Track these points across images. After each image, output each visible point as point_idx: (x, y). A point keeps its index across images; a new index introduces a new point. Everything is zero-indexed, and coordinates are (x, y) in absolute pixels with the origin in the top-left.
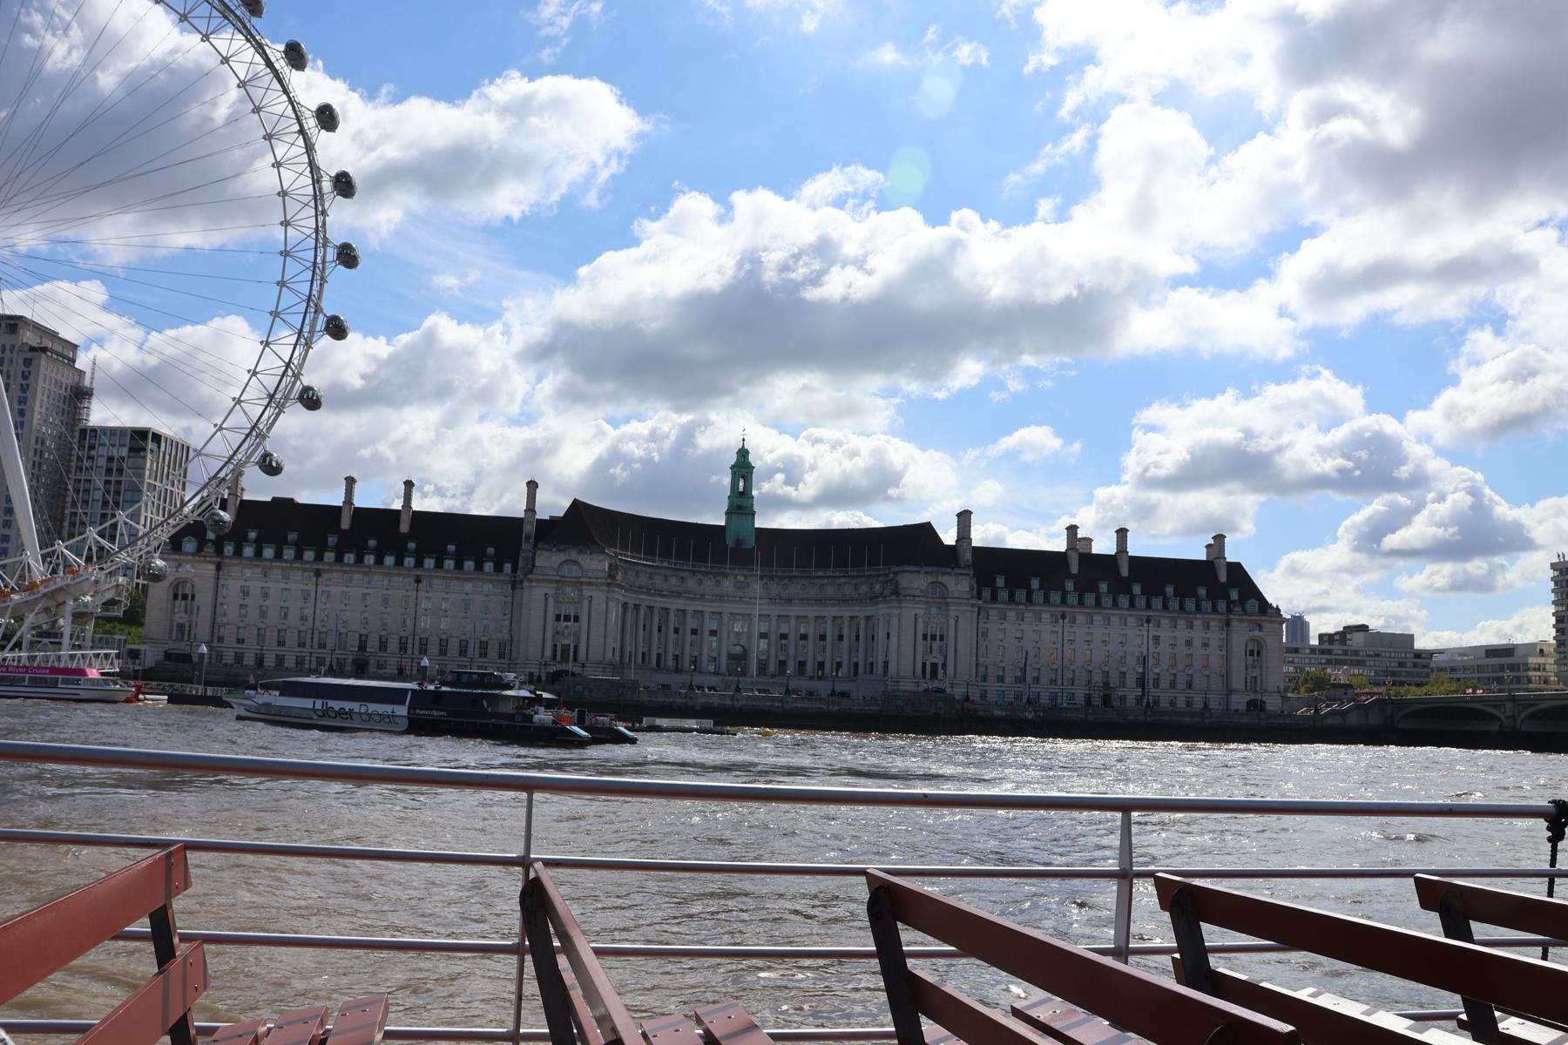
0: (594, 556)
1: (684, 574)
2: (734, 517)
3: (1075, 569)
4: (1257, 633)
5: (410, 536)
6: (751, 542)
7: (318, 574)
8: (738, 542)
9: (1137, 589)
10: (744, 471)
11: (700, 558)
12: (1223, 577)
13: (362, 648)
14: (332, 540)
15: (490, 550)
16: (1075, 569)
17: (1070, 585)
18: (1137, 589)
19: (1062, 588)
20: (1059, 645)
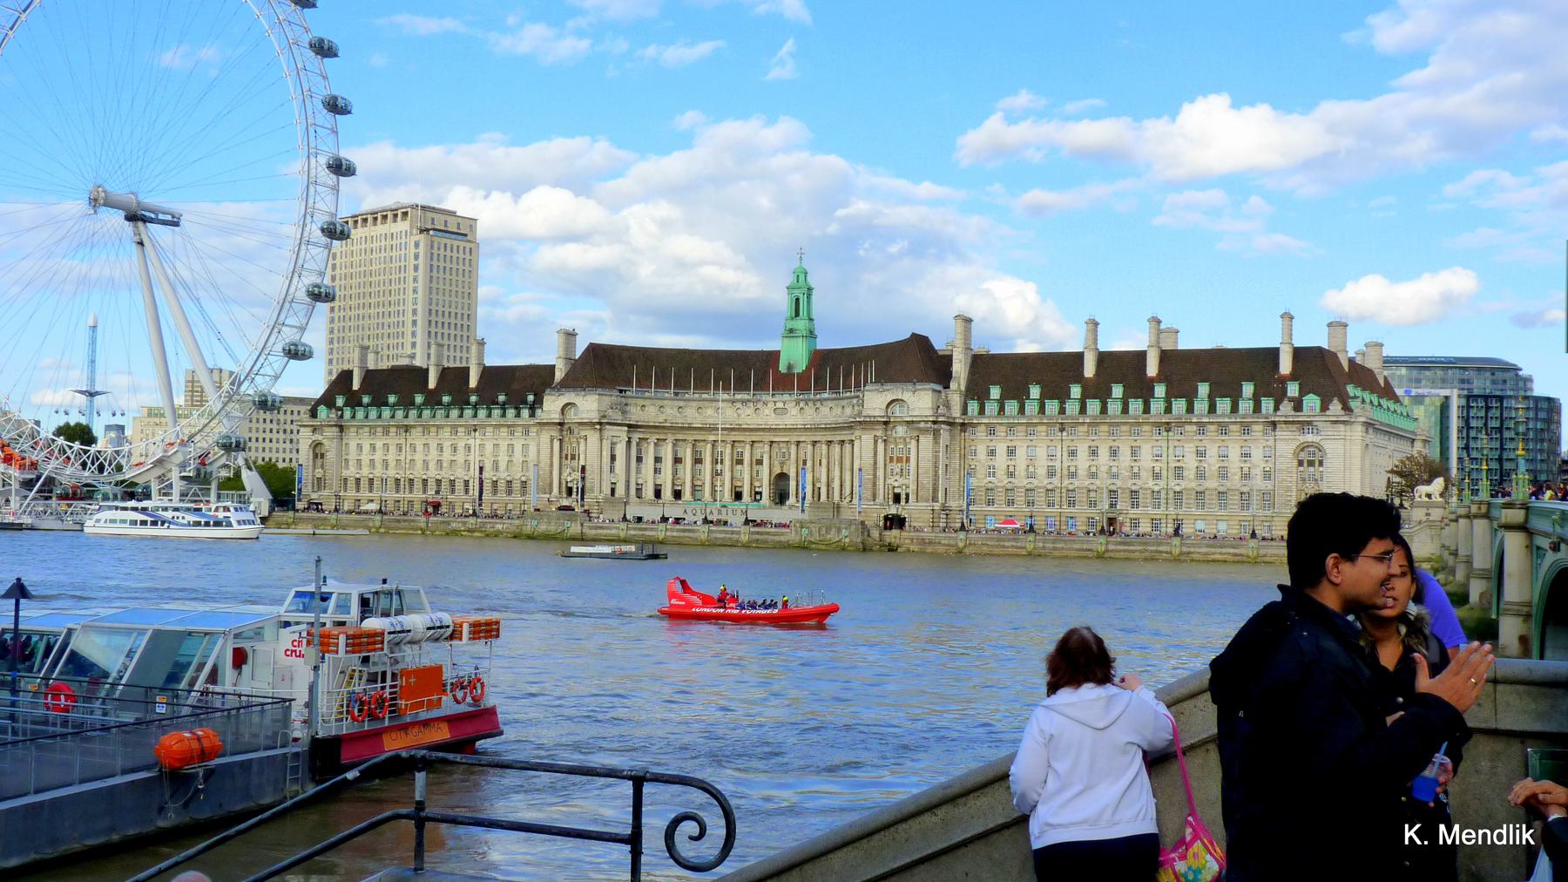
3: (1089, 370)
4: (1310, 438)
5: (476, 390)
6: (801, 365)
7: (407, 429)
8: (790, 367)
9: (1160, 390)
10: (797, 293)
11: (742, 385)
12: (1285, 366)
13: (438, 492)
14: (419, 399)
15: (531, 398)
16: (1089, 370)
17: (1076, 391)
18: (1160, 390)
19: (1063, 396)
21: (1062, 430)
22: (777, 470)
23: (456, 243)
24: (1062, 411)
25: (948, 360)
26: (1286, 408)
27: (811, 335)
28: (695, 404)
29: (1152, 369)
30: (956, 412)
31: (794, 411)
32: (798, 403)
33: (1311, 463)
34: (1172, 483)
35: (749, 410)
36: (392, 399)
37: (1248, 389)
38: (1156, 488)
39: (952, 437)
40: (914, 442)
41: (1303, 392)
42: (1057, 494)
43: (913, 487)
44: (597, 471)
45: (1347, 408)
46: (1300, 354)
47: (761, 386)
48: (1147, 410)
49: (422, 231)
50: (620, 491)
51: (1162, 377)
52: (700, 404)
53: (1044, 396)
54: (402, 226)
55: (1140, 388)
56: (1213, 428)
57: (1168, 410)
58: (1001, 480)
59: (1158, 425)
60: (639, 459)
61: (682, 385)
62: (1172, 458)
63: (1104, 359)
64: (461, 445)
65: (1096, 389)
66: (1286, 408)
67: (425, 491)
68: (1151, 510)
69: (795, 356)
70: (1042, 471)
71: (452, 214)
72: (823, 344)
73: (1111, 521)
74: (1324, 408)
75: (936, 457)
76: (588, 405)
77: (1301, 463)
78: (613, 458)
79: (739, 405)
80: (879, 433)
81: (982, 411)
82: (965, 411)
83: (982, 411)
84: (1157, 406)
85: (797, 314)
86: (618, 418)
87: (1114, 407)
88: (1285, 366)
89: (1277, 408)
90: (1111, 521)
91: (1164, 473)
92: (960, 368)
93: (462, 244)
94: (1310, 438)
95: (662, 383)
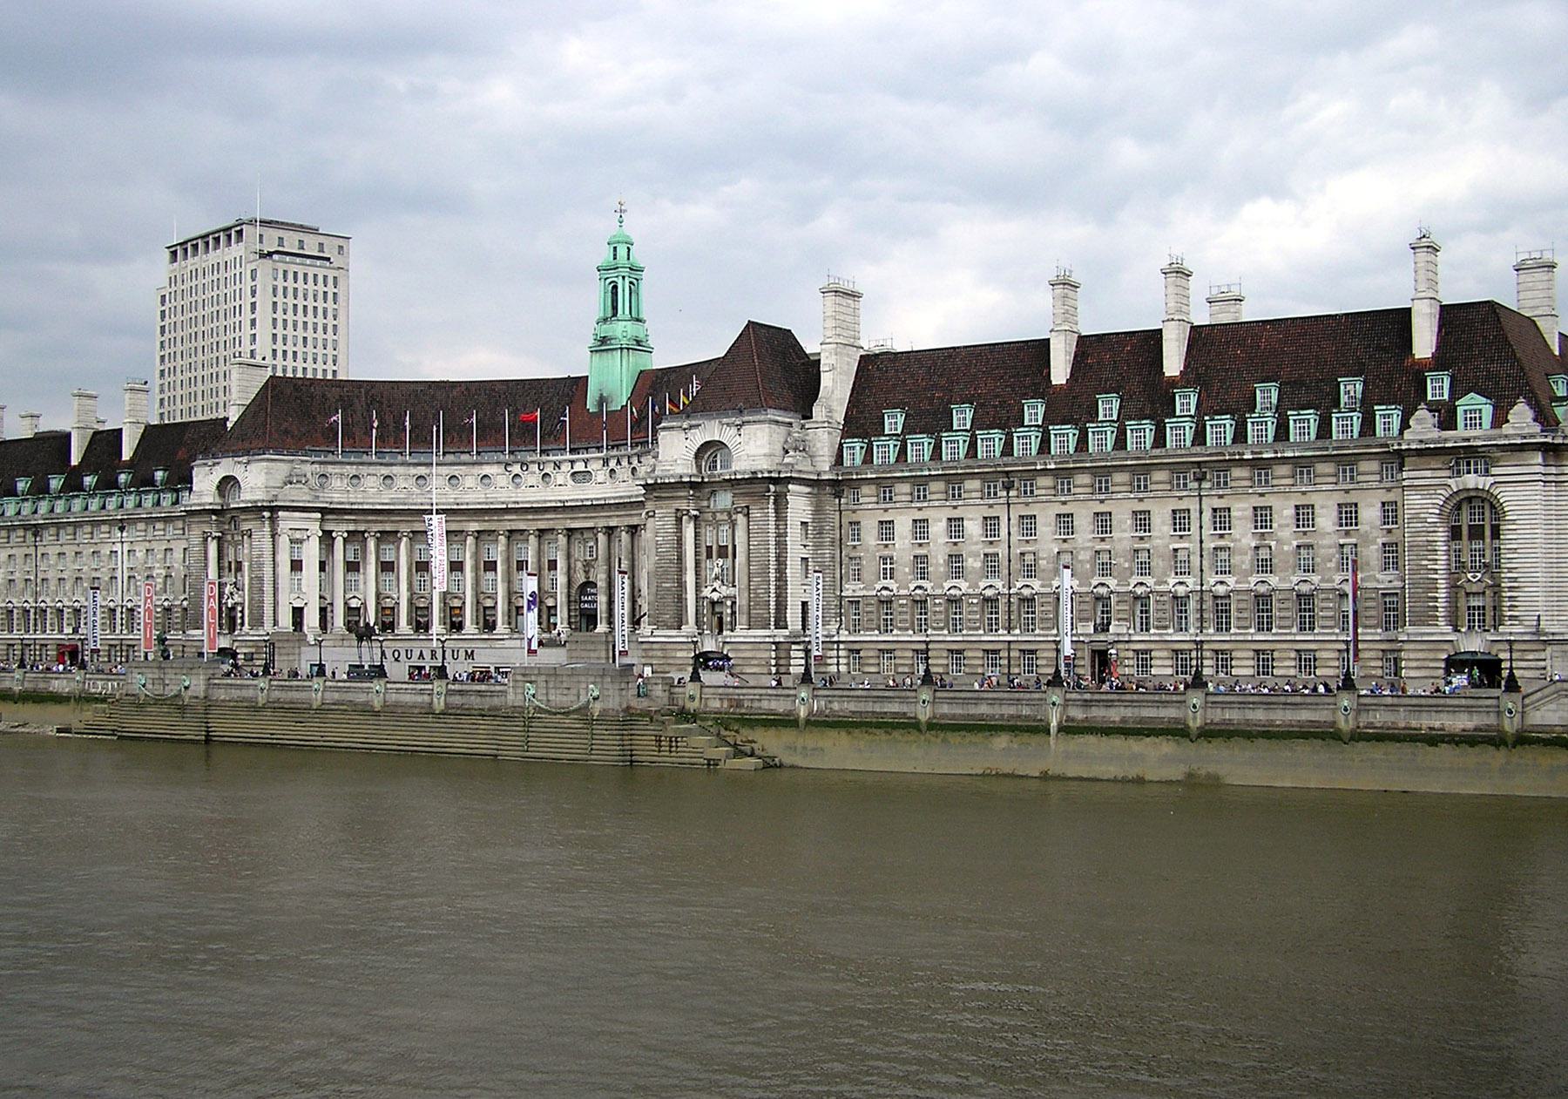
0: (253, 467)
1: (487, 470)
2: (596, 357)
3: (1060, 372)
4: (1472, 480)
5: (131, 464)
6: (621, 398)
7: (37, 530)
8: (602, 400)
12: (1424, 343)
13: (75, 631)
14: (56, 483)
16: (1060, 372)
17: (1034, 412)
18: (1185, 402)
20: (1002, 550)
21: (1008, 488)
22: (580, 578)
23: (311, 272)
24: (1008, 449)
25: (811, 368)
26: (1423, 428)
27: (639, 344)
28: (445, 470)
29: (1173, 365)
30: (824, 465)
31: (601, 475)
32: (606, 462)
33: (1476, 533)
34: (1211, 579)
35: (532, 477)
36: (22, 485)
37: (1351, 388)
38: (1181, 590)
39: (818, 510)
40: (741, 519)
41: (1456, 393)
42: (1003, 601)
43: (742, 602)
44: (268, 588)
45: (1545, 419)
46: (1452, 318)
47: (553, 438)
48: (1160, 441)
49: (263, 256)
50: (312, 619)
51: (1192, 374)
52: (455, 470)
53: (977, 423)
54: (237, 250)
55: (1154, 400)
56: (1284, 470)
57: (1200, 438)
58: (903, 585)
59: (1178, 469)
60: (352, 567)
61: (421, 440)
62: (1208, 531)
63: (1088, 347)
64: (106, 550)
65: (1071, 407)
66: (1423, 428)
67: (61, 631)
68: (1171, 635)
69: (613, 381)
70: (973, 563)
71: (314, 231)
72: (661, 359)
73: (1102, 660)
74: (1499, 420)
75: (781, 545)
76: (257, 478)
77: (1455, 533)
78: (296, 566)
79: (516, 469)
80: (683, 505)
81: (868, 458)
82: (839, 459)
83: (868, 458)
84: (1180, 431)
85: (615, 314)
86: (300, 495)
87: (1101, 440)
88: (1424, 343)
89: (1405, 425)
90: (1102, 660)
91: (1195, 560)
92: (836, 388)
93: (321, 273)
94: (1472, 480)
95: (391, 438)
